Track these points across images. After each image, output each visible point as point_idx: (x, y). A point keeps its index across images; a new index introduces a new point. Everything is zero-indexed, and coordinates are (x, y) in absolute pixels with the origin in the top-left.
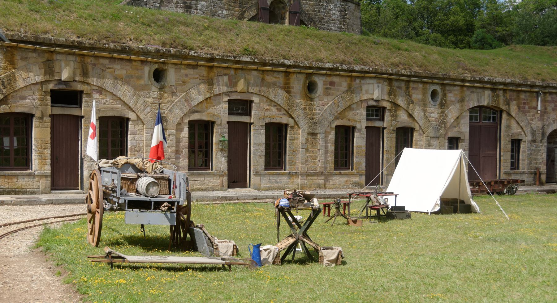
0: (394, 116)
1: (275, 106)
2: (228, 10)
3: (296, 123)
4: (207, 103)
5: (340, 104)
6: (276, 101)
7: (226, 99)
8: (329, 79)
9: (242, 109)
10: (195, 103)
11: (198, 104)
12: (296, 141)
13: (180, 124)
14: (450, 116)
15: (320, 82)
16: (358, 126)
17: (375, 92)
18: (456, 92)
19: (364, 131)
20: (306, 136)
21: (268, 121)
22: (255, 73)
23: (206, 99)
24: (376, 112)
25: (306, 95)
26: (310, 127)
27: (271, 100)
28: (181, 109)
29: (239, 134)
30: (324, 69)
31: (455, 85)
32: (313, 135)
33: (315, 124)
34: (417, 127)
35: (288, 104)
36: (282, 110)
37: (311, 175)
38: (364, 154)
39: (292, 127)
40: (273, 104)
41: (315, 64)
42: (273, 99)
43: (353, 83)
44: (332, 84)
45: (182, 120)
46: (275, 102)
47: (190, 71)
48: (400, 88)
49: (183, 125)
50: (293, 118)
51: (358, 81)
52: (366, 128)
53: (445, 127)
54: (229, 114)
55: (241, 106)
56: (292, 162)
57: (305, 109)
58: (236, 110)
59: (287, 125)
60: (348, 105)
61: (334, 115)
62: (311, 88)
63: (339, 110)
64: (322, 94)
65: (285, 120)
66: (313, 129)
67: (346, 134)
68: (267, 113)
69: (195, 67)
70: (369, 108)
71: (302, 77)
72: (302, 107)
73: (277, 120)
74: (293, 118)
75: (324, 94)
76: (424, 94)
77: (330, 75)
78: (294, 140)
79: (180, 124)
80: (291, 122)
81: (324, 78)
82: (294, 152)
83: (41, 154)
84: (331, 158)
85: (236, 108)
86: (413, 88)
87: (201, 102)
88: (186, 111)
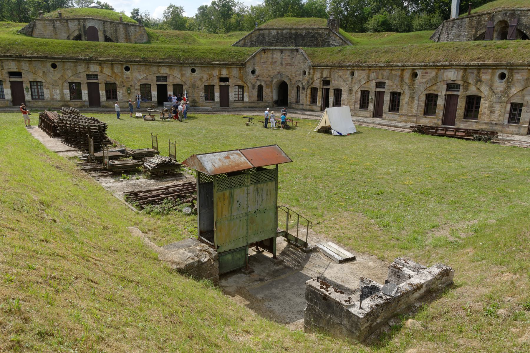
0: (466, 88)
2: (468, 32)
7: (374, 81)
8: (425, 71)
10: (362, 83)
12: (404, 100)
14: (513, 90)
15: (419, 73)
16: (439, 94)
17: (452, 75)
18: (524, 74)
19: (444, 97)
21: (391, 91)
22: (387, 70)
24: (451, 86)
29: (380, 95)
30: (420, 66)
31: (523, 69)
33: (414, 93)
34: (483, 96)
37: (409, 116)
38: (443, 108)
41: (414, 64)
43: (439, 72)
44: (426, 73)
47: (362, 72)
48: (472, 73)
51: (442, 71)
52: (445, 95)
53: (508, 96)
55: (380, 84)
56: (402, 110)
62: (415, 75)
65: (399, 91)
69: (364, 70)
70: (448, 84)
71: (410, 71)
73: (395, 90)
76: (493, 75)
77: (425, 69)
80: (402, 92)
81: (422, 71)
82: (402, 105)
83: (319, 101)
84: (423, 110)
86: (483, 73)
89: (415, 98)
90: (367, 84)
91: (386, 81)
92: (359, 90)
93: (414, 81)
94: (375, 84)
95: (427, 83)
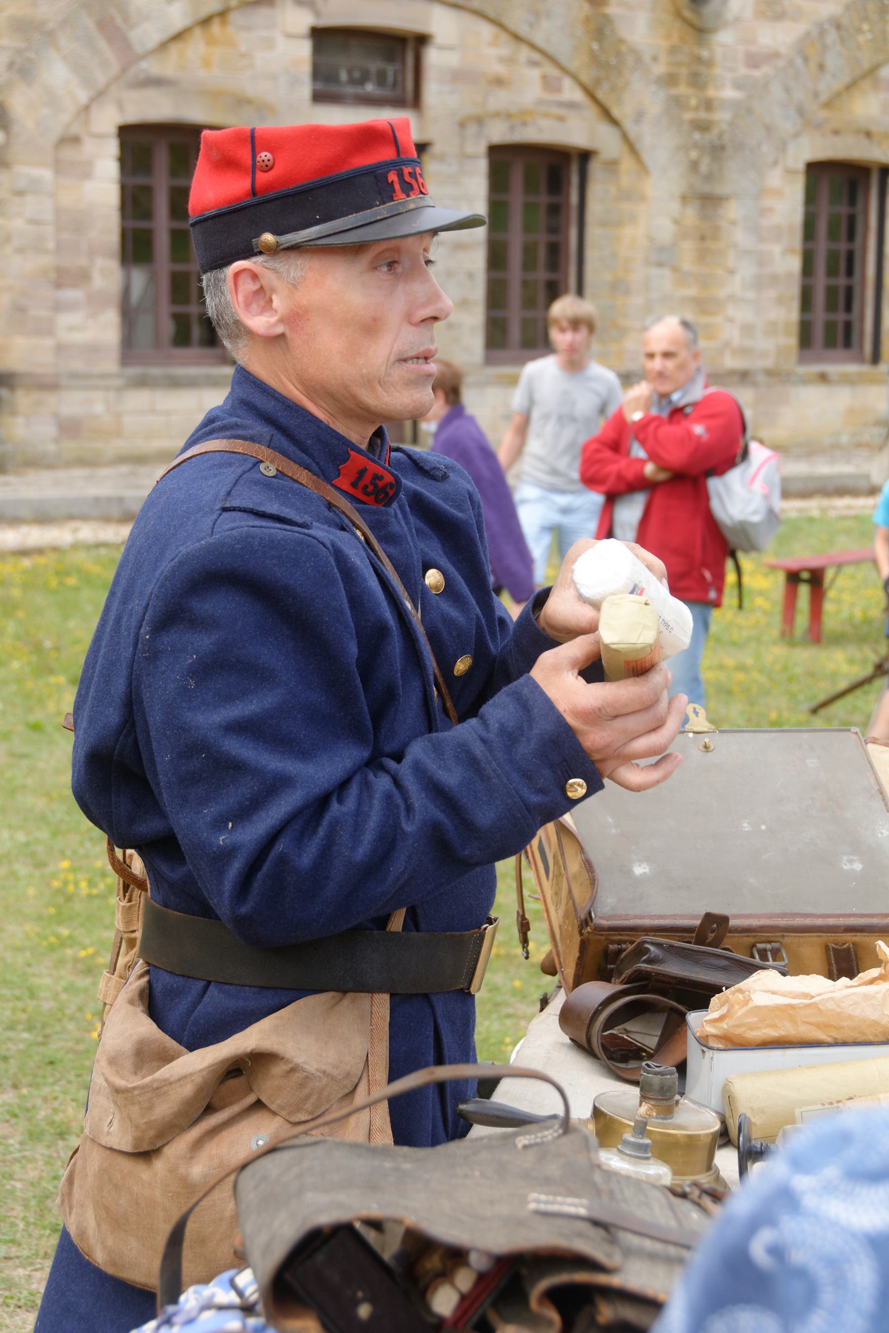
1: (534, 64)
3: (632, 149)
4: (211, 42)
5: (832, 60)
6: (539, 39)
7: (302, 20)
9: (381, 79)
10: (147, 35)
11: (164, 46)
13: (75, 140)
20: (675, 206)
21: (499, 133)
23: (206, 22)
25: (678, 14)
26: (694, 166)
27: (517, 38)
28: (78, 68)
32: (707, 201)
33: (717, 151)
35: (594, 59)
36: (567, 83)
39: (612, 165)
40: (525, 53)
42: (523, 30)
45: (87, 123)
46: (533, 46)
49: (89, 147)
50: (614, 122)
54: (318, 97)
57: (670, 80)
58: (352, 81)
59: (585, 156)
60: (866, 65)
61: (801, 111)
63: (828, 85)
64: (748, 13)
65: (575, 131)
66: (709, 178)
67: (852, 201)
68: (500, 100)
72: (660, 69)
73: (544, 132)
74: (614, 122)
75: (760, 15)
78: (619, 224)
79: (75, 140)
85: (350, 72)
87: (179, 37)
88: (101, 78)
89: (733, 211)
90: (196, 47)
91: (442, 25)
92: (108, 120)
93: (700, 32)
94: (304, 49)
95: (810, 50)
